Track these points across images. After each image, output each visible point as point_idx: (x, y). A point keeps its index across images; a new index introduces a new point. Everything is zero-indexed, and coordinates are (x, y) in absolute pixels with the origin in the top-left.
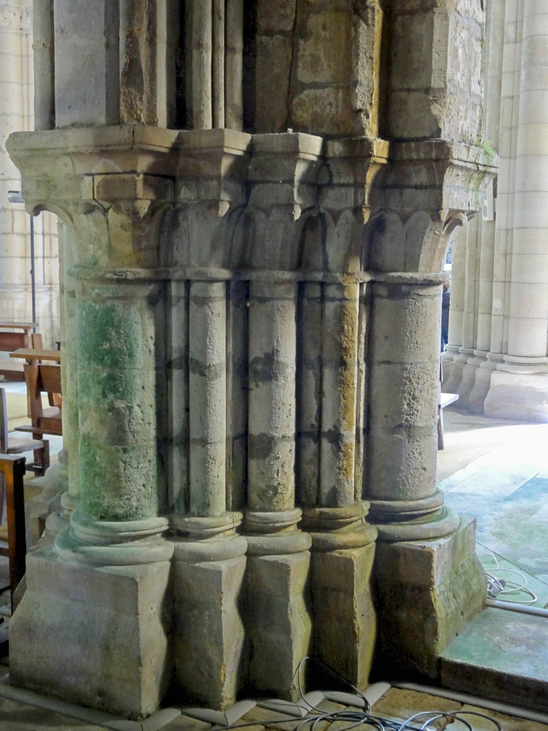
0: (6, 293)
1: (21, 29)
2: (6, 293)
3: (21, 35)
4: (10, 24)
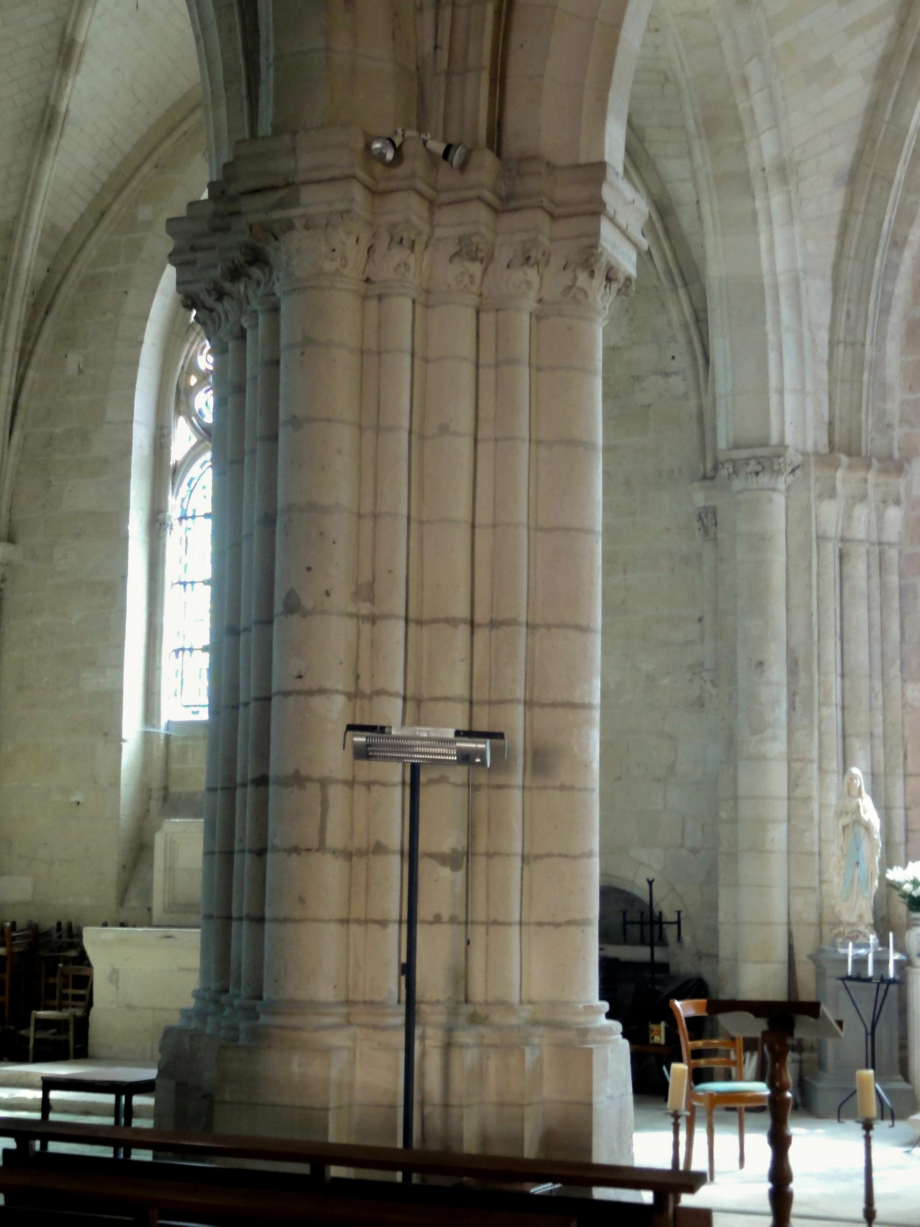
0: (299, 1028)
1: (368, 280)
2: (299, 1028)
3: (365, 298)
4: (344, 266)
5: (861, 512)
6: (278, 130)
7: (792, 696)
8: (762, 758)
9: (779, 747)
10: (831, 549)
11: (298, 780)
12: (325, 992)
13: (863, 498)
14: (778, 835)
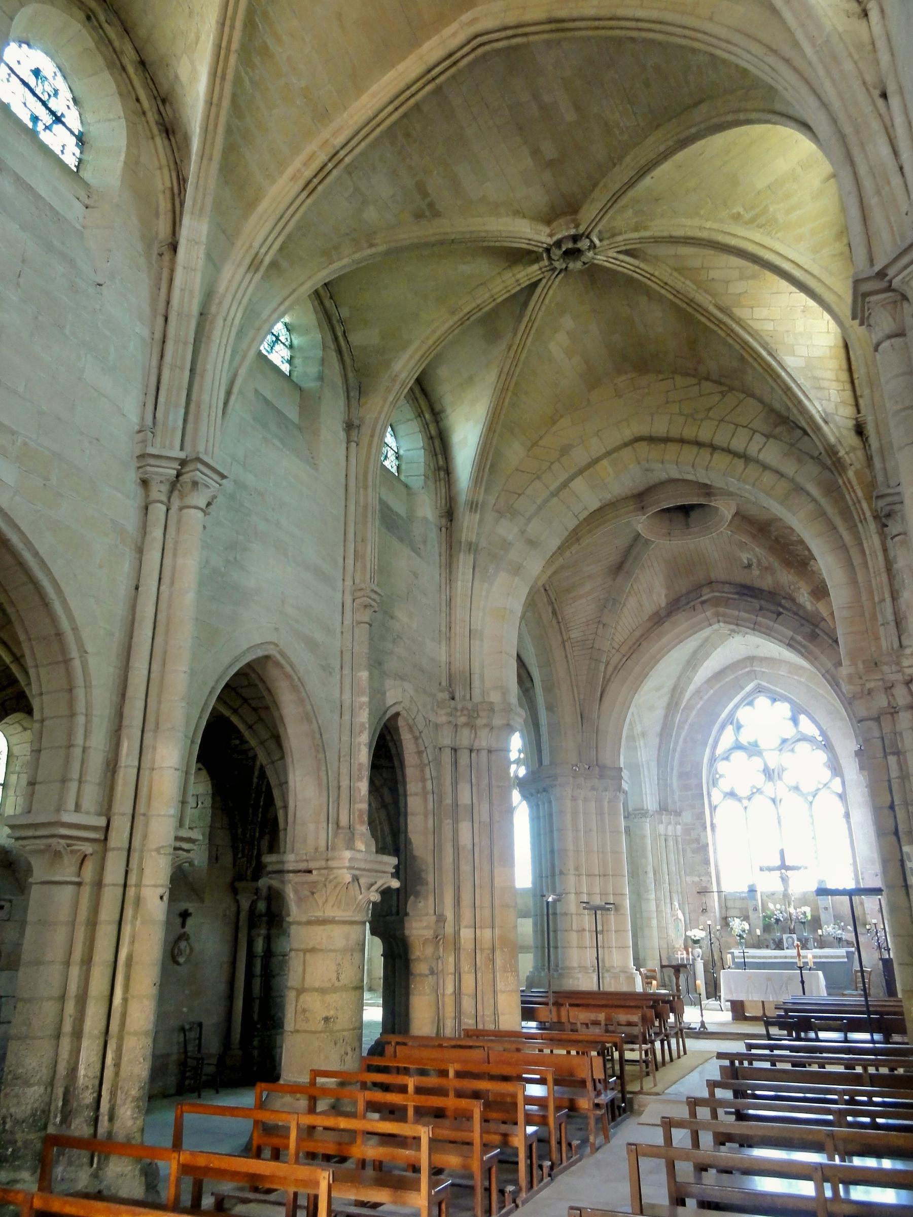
5: (670, 828)
6: (552, 763)
7: (655, 881)
8: (648, 899)
9: (653, 896)
10: (663, 838)
11: (566, 914)
12: (575, 964)
13: (670, 823)
14: (654, 922)
